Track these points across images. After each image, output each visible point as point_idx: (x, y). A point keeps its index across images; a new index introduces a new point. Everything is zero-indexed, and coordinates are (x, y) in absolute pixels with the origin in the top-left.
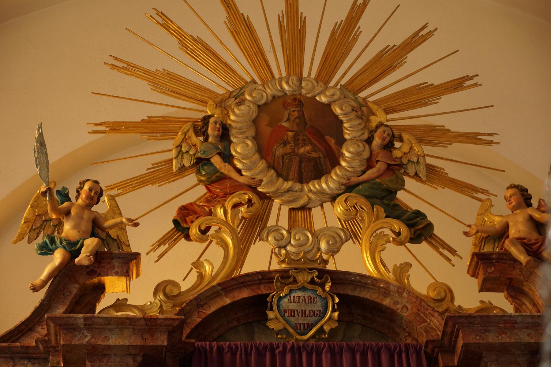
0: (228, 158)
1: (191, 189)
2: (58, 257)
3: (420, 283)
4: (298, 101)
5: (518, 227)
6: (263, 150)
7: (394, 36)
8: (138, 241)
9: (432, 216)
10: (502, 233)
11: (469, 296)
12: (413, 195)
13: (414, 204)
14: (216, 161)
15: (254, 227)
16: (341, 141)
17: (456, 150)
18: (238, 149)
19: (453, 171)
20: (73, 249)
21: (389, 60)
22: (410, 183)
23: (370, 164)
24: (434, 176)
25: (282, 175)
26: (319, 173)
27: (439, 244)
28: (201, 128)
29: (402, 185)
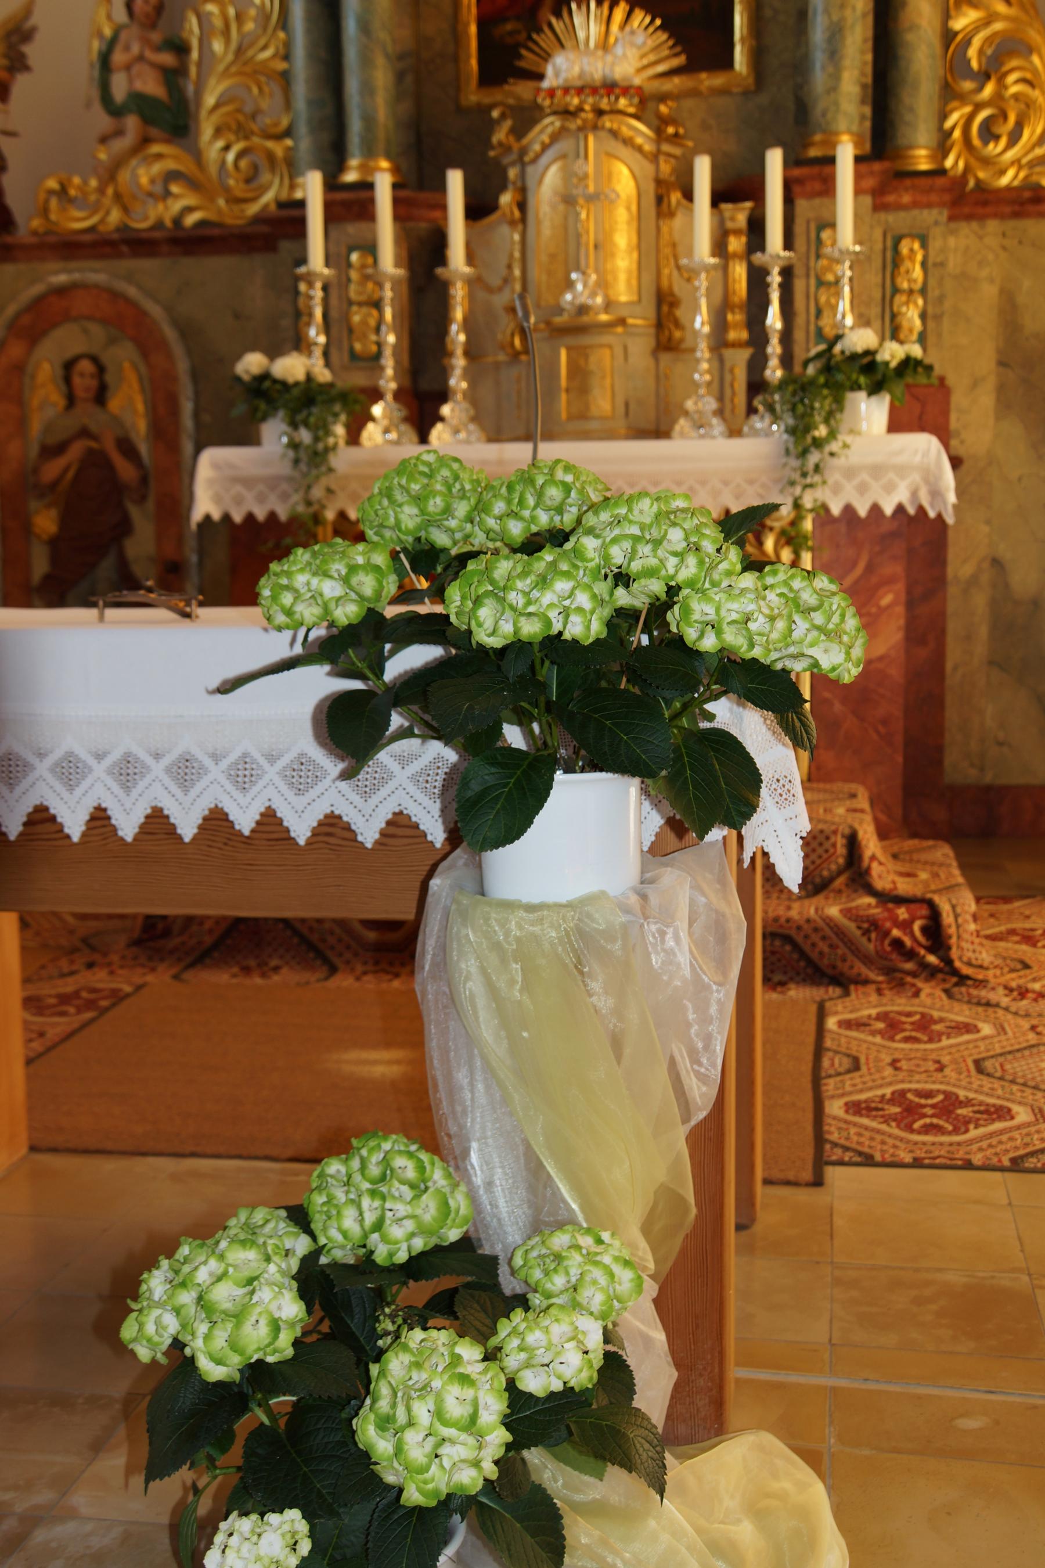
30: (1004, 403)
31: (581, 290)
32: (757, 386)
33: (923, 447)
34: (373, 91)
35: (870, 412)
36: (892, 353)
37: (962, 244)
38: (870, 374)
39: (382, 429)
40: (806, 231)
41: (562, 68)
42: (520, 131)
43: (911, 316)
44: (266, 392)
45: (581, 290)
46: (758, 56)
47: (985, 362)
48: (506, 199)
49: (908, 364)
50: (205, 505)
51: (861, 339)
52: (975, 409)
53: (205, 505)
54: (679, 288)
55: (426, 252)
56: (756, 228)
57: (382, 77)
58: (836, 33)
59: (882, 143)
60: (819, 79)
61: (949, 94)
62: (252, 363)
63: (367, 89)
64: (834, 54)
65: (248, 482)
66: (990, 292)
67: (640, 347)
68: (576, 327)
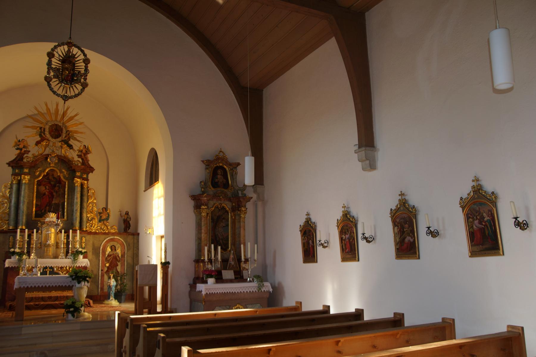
0: (44, 134)
1: (39, 139)
2: (18, 151)
3: (70, 157)
4: (56, 125)
5: (84, 151)
6: (50, 133)
7: (72, 114)
8: (30, 148)
9: (74, 146)
10: (82, 151)
11: (76, 158)
12: (72, 142)
13: (72, 144)
14: (43, 134)
15: (47, 146)
16: (62, 132)
17: (79, 135)
18: (46, 133)
19: (78, 138)
20: (21, 149)
21: (71, 118)
22: (71, 140)
23: (66, 137)
24: (75, 139)
25: (52, 137)
26: (58, 138)
27: (74, 150)
28: (41, 128)
29: (70, 140)
30: (93, 253)
31: (49, 242)
32: (67, 252)
33: (86, 260)
34: (23, 218)
35: (81, 257)
36: (83, 251)
37: (89, 237)
38: (81, 253)
39: (24, 257)
40: (74, 237)
41: (47, 220)
42: (42, 225)
43: (84, 245)
44: (14, 253)
45: (49, 242)
46: (67, 217)
47: (91, 249)
48: (40, 231)
49: (85, 252)
50: (7, 265)
51: (80, 250)
52: (90, 254)
53: (7, 265)
54: (59, 242)
55: (30, 236)
56: (68, 237)
57: (24, 217)
58: (76, 218)
59: (81, 228)
60: (75, 222)
61: (87, 222)
62: (12, 250)
63: (23, 219)
64: (76, 219)
65: (12, 263)
66: (91, 242)
67: (55, 248)
68: (49, 245)
